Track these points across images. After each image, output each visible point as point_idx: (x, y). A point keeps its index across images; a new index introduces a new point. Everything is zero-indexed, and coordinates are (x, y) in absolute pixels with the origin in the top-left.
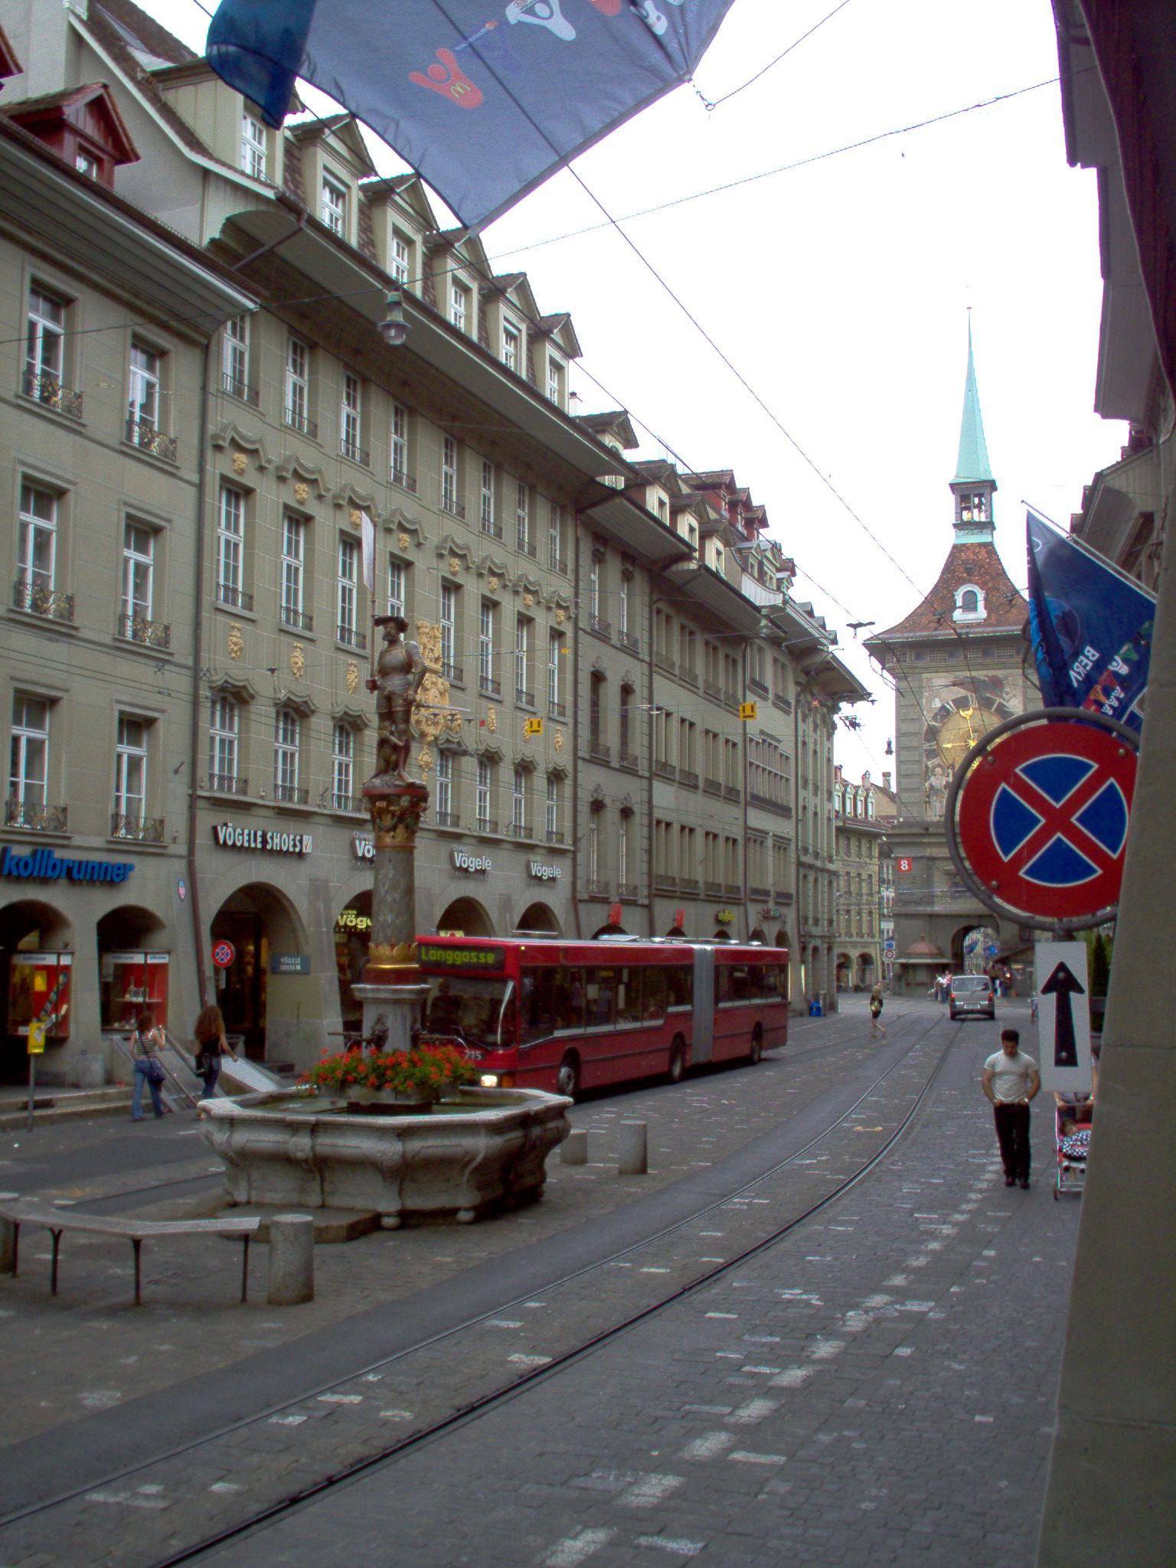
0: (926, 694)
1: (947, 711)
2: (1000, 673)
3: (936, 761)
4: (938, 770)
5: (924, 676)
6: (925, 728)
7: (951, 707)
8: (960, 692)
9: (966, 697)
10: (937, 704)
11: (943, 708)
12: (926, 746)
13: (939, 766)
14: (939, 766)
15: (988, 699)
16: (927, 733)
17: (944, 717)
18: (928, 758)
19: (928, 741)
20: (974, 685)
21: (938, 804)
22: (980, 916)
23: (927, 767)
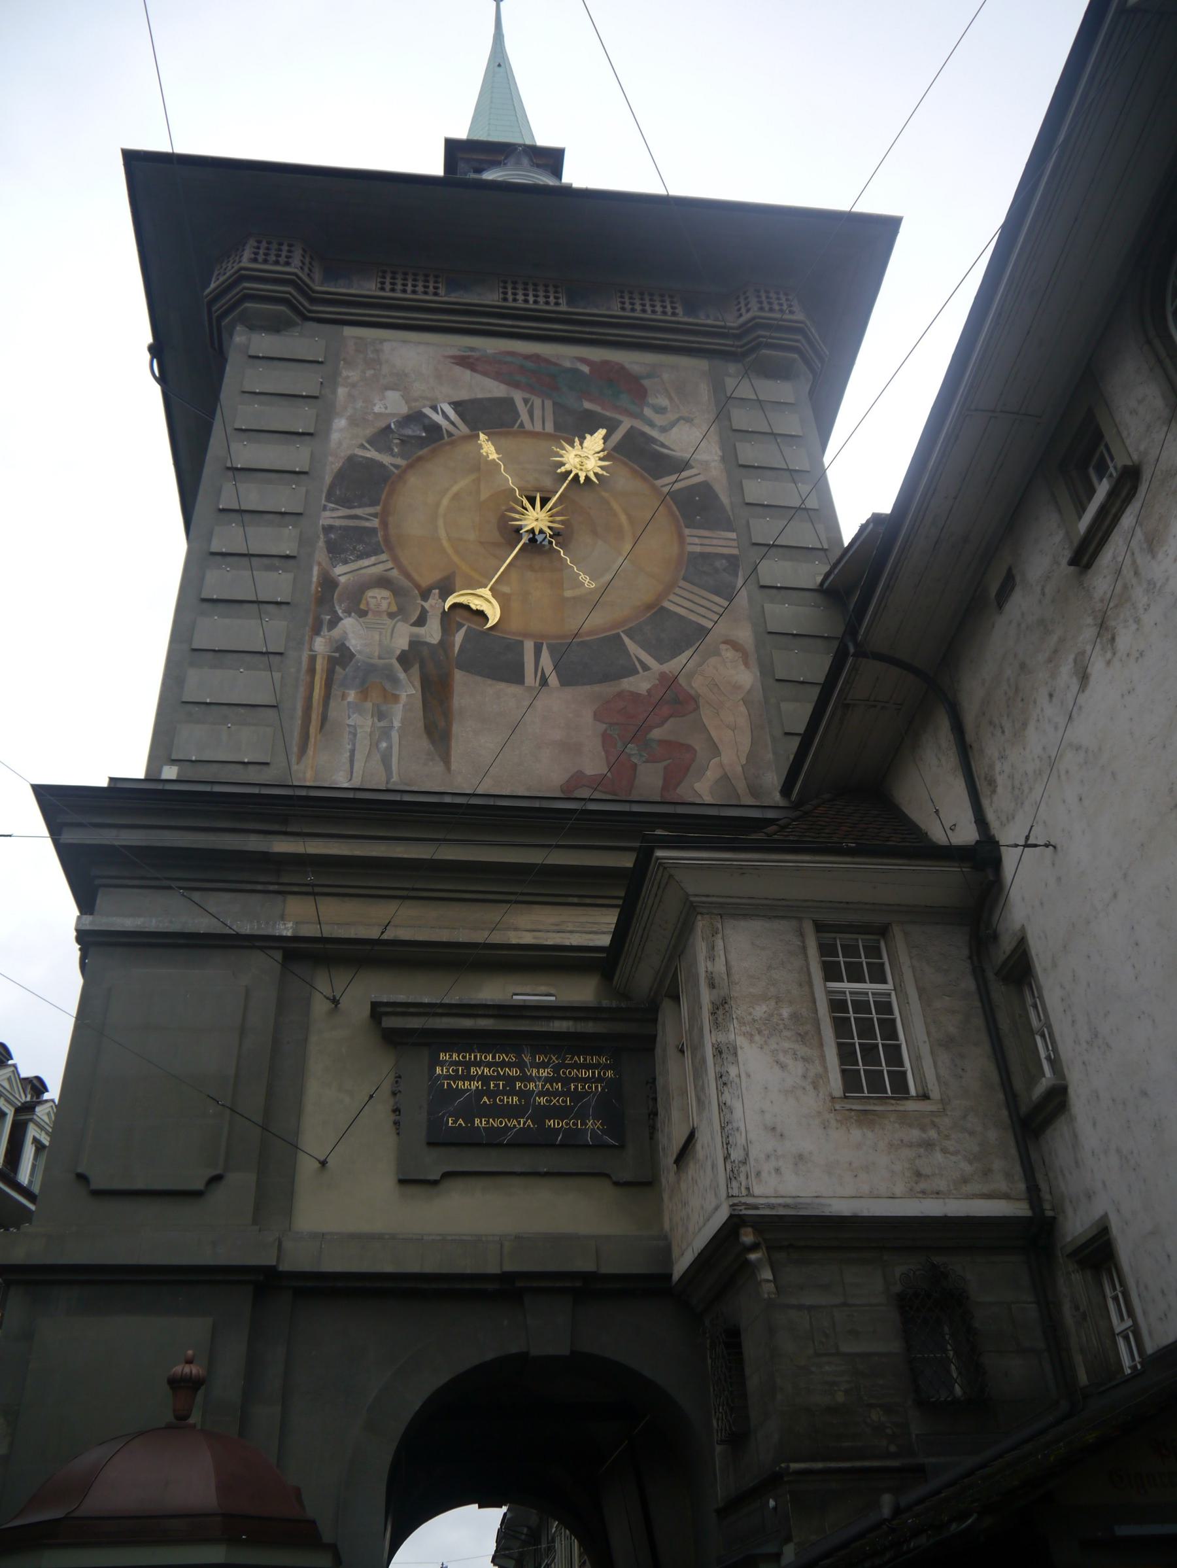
0: (351, 374)
1: (434, 430)
2: (633, 361)
3: (373, 566)
4: (379, 598)
5: (349, 331)
6: (333, 465)
7: (445, 416)
8: (491, 388)
9: (508, 403)
10: (392, 405)
11: (416, 417)
12: (332, 516)
13: (383, 582)
14: (383, 582)
15: (587, 411)
16: (340, 476)
17: (422, 442)
18: (336, 551)
19: (345, 502)
20: (543, 380)
21: (364, 723)
22: (586, 1289)
23: (328, 583)
